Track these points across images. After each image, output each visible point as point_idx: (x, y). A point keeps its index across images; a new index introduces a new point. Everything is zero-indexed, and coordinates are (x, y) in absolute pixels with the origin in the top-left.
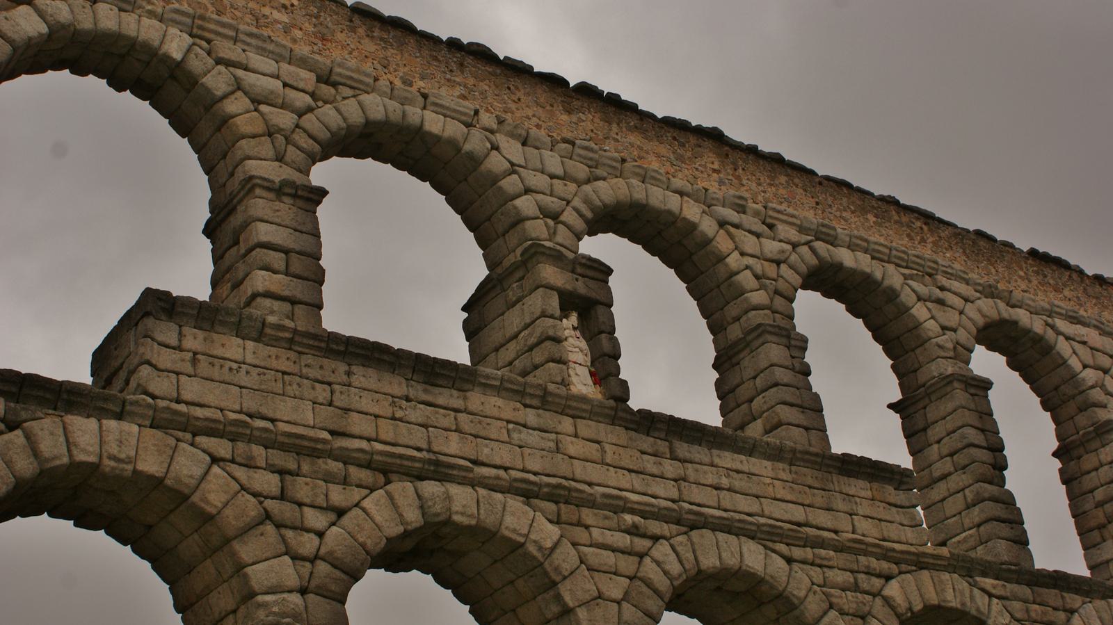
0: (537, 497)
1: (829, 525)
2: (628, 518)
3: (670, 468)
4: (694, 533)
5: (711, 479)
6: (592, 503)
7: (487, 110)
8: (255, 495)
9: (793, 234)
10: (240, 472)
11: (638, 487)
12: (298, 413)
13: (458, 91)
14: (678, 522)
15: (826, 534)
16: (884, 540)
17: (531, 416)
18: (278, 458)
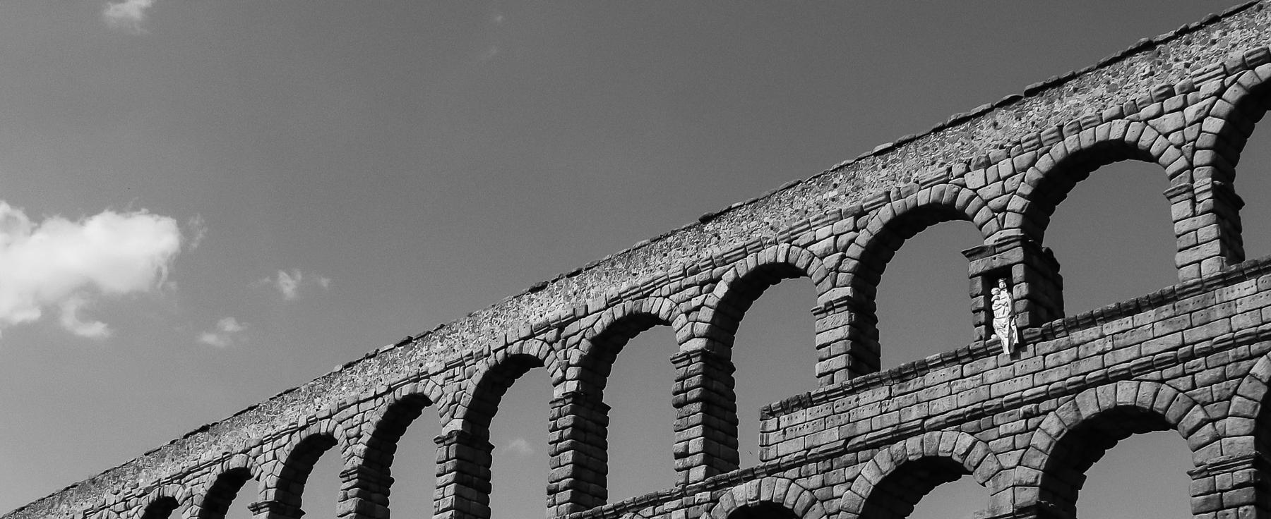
0: (965, 421)
1: (1205, 336)
2: (1021, 410)
3: (1065, 356)
4: (1078, 398)
5: (1099, 349)
6: (1000, 409)
7: (960, 161)
8: (810, 491)
9: (1214, 85)
10: (803, 482)
11: (1037, 382)
12: (831, 437)
13: (941, 160)
14: (1066, 393)
15: (1197, 347)
16: (1263, 323)
17: (967, 370)
18: (821, 465)
